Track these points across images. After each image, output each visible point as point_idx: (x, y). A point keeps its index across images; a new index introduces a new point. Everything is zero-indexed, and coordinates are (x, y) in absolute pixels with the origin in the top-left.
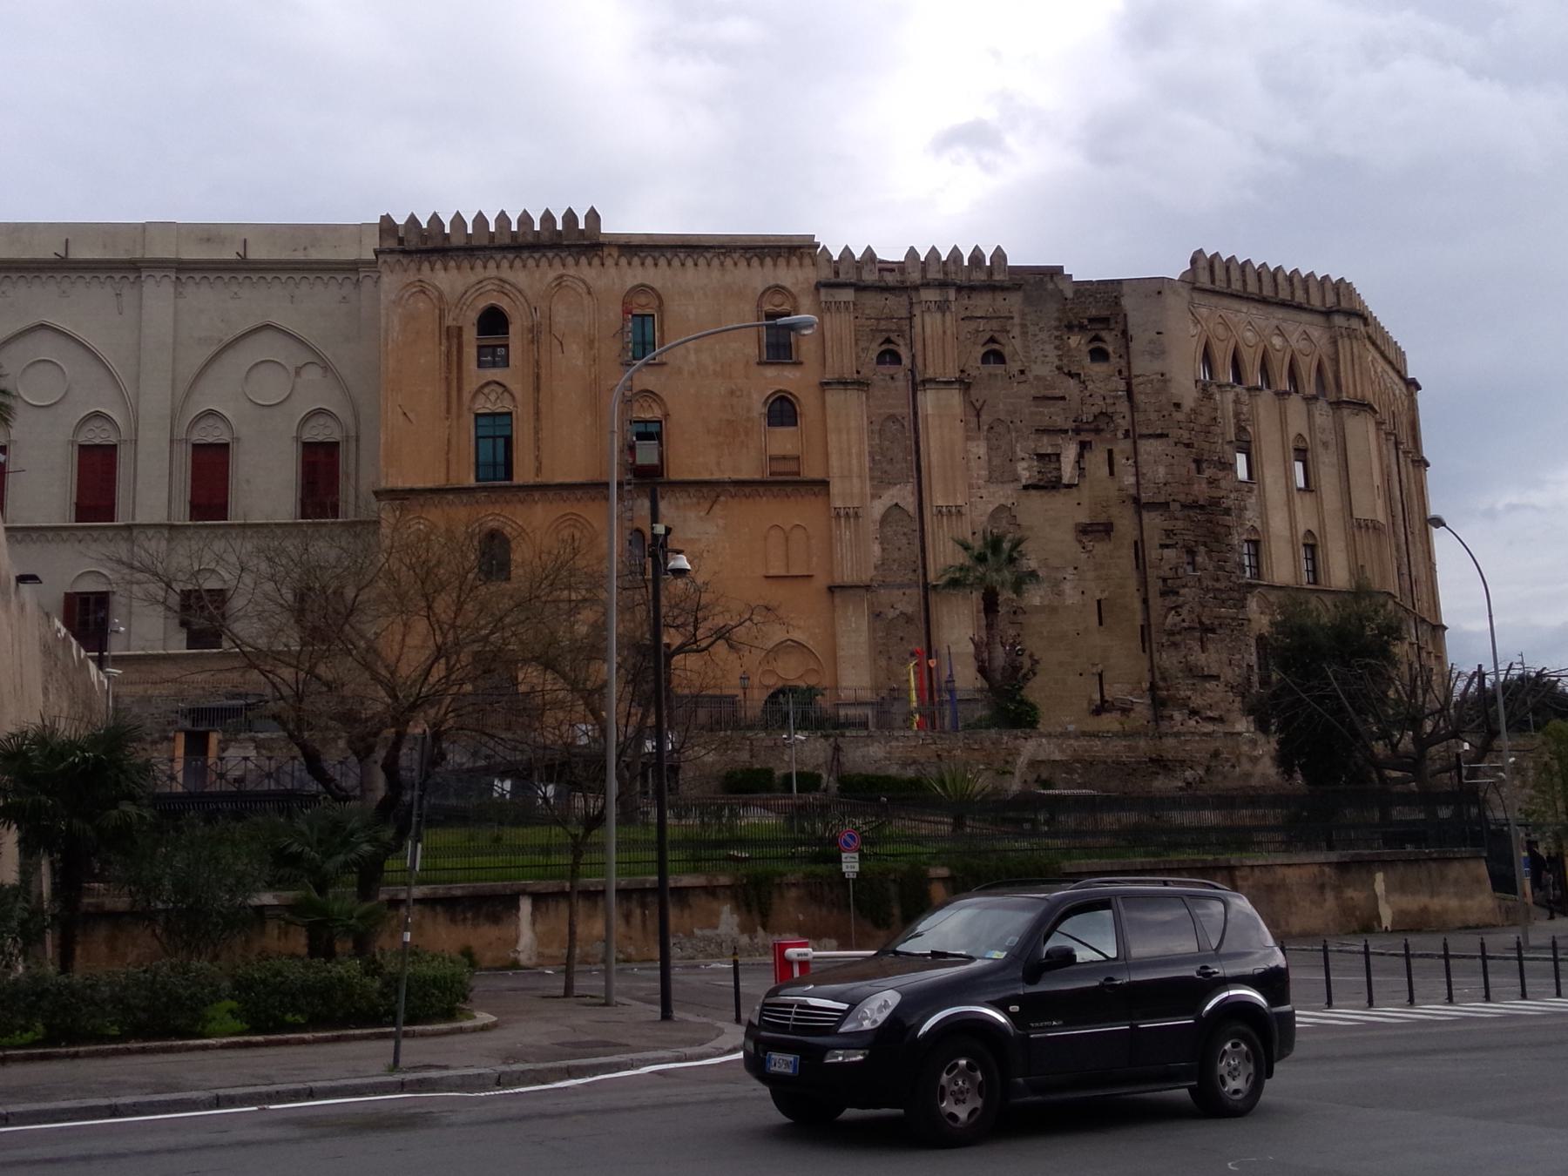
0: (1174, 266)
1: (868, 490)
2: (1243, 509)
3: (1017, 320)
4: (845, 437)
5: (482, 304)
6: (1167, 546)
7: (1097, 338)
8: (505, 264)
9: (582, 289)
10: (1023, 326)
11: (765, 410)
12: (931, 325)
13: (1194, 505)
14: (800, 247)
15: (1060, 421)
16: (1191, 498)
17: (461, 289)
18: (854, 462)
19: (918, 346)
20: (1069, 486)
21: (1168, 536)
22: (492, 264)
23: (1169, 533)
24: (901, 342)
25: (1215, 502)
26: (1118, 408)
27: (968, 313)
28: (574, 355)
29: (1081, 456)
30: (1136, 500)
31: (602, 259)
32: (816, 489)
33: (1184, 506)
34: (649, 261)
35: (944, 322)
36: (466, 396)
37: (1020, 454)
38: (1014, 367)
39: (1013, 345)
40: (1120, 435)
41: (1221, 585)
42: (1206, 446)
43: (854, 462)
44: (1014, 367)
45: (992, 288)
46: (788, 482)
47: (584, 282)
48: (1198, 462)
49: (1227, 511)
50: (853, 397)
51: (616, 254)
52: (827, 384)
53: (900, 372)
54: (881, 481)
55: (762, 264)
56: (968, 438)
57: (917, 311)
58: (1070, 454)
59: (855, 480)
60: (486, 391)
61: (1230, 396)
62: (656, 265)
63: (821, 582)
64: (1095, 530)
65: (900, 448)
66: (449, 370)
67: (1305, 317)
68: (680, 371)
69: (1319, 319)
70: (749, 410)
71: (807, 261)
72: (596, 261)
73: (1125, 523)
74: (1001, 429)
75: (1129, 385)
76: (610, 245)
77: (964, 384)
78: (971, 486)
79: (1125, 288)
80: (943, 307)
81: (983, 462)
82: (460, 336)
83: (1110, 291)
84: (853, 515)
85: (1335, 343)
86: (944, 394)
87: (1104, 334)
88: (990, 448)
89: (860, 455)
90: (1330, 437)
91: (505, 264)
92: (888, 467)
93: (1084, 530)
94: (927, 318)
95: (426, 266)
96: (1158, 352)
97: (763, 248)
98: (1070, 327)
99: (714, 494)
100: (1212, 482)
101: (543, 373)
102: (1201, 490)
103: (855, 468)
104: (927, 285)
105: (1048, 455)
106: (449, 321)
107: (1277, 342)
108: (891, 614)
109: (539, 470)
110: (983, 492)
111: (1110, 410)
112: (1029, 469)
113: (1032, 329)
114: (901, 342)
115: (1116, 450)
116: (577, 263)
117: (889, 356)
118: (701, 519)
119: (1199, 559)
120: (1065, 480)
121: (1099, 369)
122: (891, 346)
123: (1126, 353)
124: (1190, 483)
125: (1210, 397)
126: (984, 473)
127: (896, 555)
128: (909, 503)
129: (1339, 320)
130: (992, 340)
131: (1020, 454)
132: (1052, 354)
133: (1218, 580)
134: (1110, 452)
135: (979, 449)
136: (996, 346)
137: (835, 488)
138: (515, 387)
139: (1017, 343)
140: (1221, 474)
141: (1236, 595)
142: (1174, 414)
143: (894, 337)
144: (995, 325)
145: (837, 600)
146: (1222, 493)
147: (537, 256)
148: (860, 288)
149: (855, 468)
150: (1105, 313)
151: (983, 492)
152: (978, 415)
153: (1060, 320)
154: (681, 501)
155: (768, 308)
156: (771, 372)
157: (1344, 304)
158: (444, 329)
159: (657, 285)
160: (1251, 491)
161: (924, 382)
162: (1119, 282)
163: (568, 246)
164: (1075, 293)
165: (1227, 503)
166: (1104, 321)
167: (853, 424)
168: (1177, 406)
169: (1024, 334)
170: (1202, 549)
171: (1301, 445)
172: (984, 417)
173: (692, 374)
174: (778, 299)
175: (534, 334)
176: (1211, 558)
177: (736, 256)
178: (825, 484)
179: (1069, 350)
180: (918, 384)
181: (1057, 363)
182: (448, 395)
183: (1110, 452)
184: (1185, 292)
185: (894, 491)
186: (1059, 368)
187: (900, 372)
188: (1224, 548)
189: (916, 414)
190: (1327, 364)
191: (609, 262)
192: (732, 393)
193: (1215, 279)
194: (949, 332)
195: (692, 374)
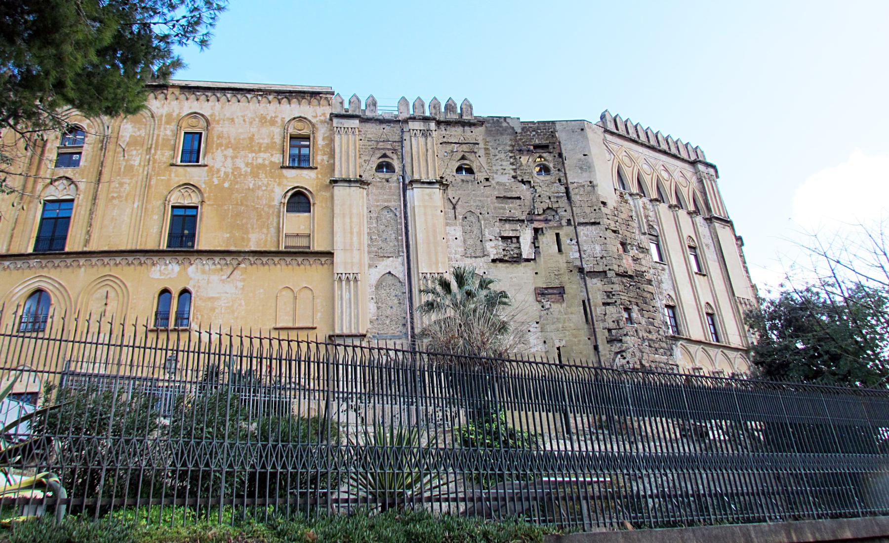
1: (366, 260)
2: (660, 282)
3: (482, 145)
4: (348, 220)
6: (608, 304)
10: (486, 149)
12: (416, 145)
13: (624, 275)
14: (319, 93)
16: (621, 270)
18: (355, 239)
19: (407, 160)
20: (528, 260)
21: (608, 296)
23: (609, 294)
24: (395, 157)
26: (560, 204)
27: (445, 140)
29: (535, 238)
30: (581, 270)
31: (166, 95)
32: (323, 260)
33: (617, 275)
37: (488, 236)
39: (478, 162)
40: (564, 222)
41: (654, 336)
42: (628, 234)
43: (355, 239)
44: (480, 176)
45: (462, 123)
48: (623, 244)
50: (355, 192)
52: (336, 181)
54: (379, 255)
56: (447, 224)
57: (406, 136)
58: (526, 236)
59: (356, 252)
60: (57, 183)
62: (208, 100)
64: (550, 293)
71: (323, 102)
73: (573, 286)
74: (472, 219)
75: (567, 189)
78: (450, 259)
79: (558, 127)
80: (426, 134)
81: (460, 241)
83: (548, 128)
85: (701, 181)
86: (428, 191)
89: (359, 234)
92: (383, 245)
93: (541, 293)
96: (586, 166)
97: (290, 92)
98: (520, 151)
100: (635, 260)
102: (627, 263)
104: (413, 119)
105: (511, 238)
109: (87, 242)
111: (555, 206)
112: (495, 247)
113: (492, 151)
115: (561, 233)
117: (385, 166)
118: (223, 281)
119: (635, 315)
120: (524, 256)
124: (620, 258)
126: (461, 250)
127: (389, 312)
128: (399, 270)
129: (701, 167)
132: (509, 168)
133: (650, 332)
134: (557, 235)
135: (456, 231)
137: (337, 258)
139: (483, 160)
140: (641, 256)
142: (602, 208)
143: (389, 153)
146: (644, 269)
148: (364, 120)
150: (544, 142)
152: (454, 208)
154: (207, 267)
155: (291, 130)
157: (700, 159)
161: (412, 182)
162: (553, 122)
164: (523, 129)
165: (648, 276)
166: (545, 147)
168: (604, 203)
169: (487, 154)
170: (635, 308)
174: (300, 125)
176: (643, 316)
177: (271, 97)
178: (330, 254)
179: (521, 165)
180: (407, 185)
183: (557, 235)
186: (514, 177)
188: (652, 309)
190: (698, 194)
193: (616, 130)
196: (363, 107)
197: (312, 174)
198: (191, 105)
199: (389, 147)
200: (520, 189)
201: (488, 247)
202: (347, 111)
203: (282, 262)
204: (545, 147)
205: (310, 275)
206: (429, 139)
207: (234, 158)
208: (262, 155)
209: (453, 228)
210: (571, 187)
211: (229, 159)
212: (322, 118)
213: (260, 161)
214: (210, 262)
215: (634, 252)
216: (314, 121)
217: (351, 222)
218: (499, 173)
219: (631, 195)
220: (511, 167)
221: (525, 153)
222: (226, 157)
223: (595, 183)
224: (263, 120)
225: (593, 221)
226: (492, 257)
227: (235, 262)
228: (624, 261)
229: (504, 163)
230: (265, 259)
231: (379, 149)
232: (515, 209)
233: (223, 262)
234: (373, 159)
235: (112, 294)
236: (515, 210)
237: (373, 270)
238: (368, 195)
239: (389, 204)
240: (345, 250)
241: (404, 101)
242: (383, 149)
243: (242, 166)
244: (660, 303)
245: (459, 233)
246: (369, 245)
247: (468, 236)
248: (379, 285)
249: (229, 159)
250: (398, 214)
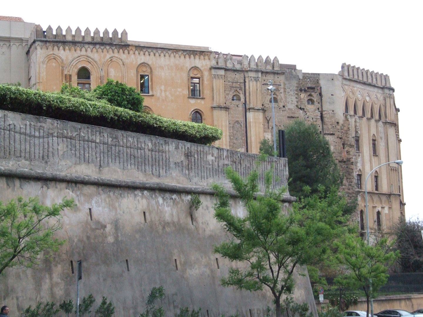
2: (357, 163)
3: (282, 86)
5: (80, 66)
7: (310, 95)
8: (89, 50)
9: (121, 63)
10: (285, 89)
12: (252, 86)
14: (204, 52)
17: (70, 59)
22: (83, 49)
24: (241, 92)
25: (349, 160)
27: (265, 82)
33: (340, 162)
34: (147, 53)
38: (281, 105)
39: (281, 96)
41: (351, 191)
47: (121, 60)
48: (343, 144)
49: (352, 163)
50: (223, 113)
51: (134, 50)
52: (214, 107)
53: (241, 104)
55: (190, 58)
56: (265, 131)
57: (247, 80)
61: (353, 120)
62: (149, 55)
67: (376, 90)
68: (159, 99)
69: (380, 91)
72: (126, 51)
75: (322, 114)
76: (132, 46)
79: (321, 77)
80: (256, 79)
82: (70, 79)
83: (315, 78)
85: (385, 99)
86: (257, 114)
87: (313, 94)
90: (382, 135)
91: (89, 50)
95: (56, 48)
98: (301, 90)
104: (251, 71)
106: (66, 72)
107: (368, 99)
113: (288, 90)
114: (241, 92)
116: (119, 52)
117: (235, 97)
122: (237, 94)
125: (348, 120)
129: (386, 91)
132: (295, 100)
133: (349, 189)
139: (282, 95)
140: (351, 149)
141: (354, 195)
142: (337, 126)
143: (238, 90)
146: (351, 156)
147: (102, 47)
150: (313, 86)
152: (268, 123)
153: (297, 87)
155: (192, 75)
156: (192, 101)
157: (388, 85)
158: (64, 76)
159: (150, 63)
160: (359, 156)
161: (249, 109)
162: (319, 74)
163: (115, 45)
164: (303, 77)
167: (224, 124)
168: (338, 123)
169: (285, 91)
171: (374, 138)
172: (270, 124)
174: (196, 72)
177: (180, 53)
179: (301, 99)
181: (296, 104)
184: (340, 78)
186: (297, 106)
190: (382, 107)
191: (131, 52)
194: (258, 90)
197: (203, 102)
199: (238, 86)
206: (258, 82)
208: (179, 90)
209: (267, 133)
210: (324, 113)
211: (163, 92)
212: (206, 67)
213: (178, 93)
215: (347, 149)
216: (202, 69)
219: (350, 116)
221: (303, 91)
222: (161, 90)
223: (335, 112)
225: (332, 133)
228: (343, 154)
231: (233, 87)
234: (231, 93)
239: (238, 120)
242: (235, 87)
244: (355, 174)
246: (229, 141)
249: (163, 92)
250: (242, 125)
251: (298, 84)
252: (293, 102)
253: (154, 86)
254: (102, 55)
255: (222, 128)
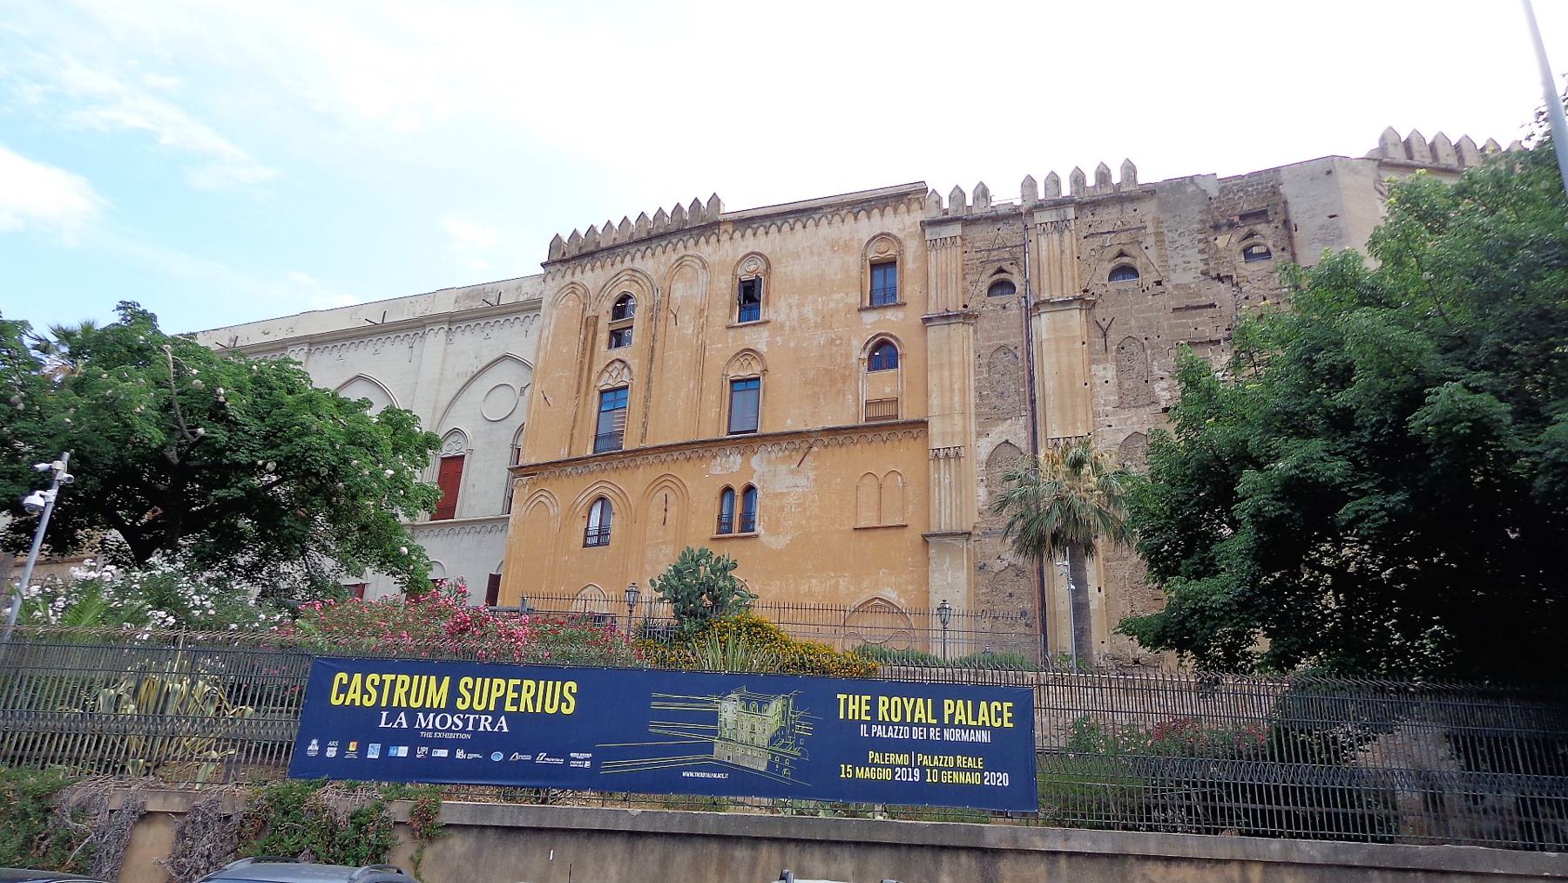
0: (1359, 144)
3: (1150, 229)
4: (946, 373)
5: (616, 293)
9: (697, 265)
10: (1159, 234)
11: (865, 356)
12: (1045, 247)
14: (907, 194)
15: (1208, 332)
18: (956, 399)
19: (1032, 272)
22: (628, 258)
24: (1015, 270)
27: (1092, 230)
28: (687, 326)
32: (915, 432)
35: (1061, 241)
36: (594, 377)
39: (1147, 257)
43: (956, 399)
44: (1148, 279)
45: (1121, 198)
46: (885, 425)
47: (700, 258)
50: (959, 331)
52: (929, 320)
54: (989, 416)
56: (1092, 362)
59: (958, 420)
63: (916, 531)
65: (1015, 383)
66: (584, 355)
68: (782, 327)
70: (848, 356)
71: (915, 206)
72: (713, 239)
74: (1134, 348)
77: (1085, 301)
79: (1284, 176)
80: (1060, 227)
84: (954, 456)
88: (1120, 371)
89: (963, 391)
92: (996, 402)
94: (1043, 241)
97: (868, 200)
98: (1217, 227)
99: (805, 446)
101: (658, 346)
103: (957, 407)
106: (589, 313)
108: (998, 566)
109: (644, 436)
110: (1113, 420)
113: (1169, 236)
117: (1001, 286)
118: (792, 472)
121: (1255, 267)
123: (1289, 245)
126: (1114, 398)
128: (1021, 439)
130: (1122, 254)
131: (1158, 373)
136: (1125, 260)
137: (935, 427)
138: (634, 363)
139: (1152, 254)
144: (1124, 238)
145: (932, 552)
148: (969, 222)
149: (957, 407)
150: (1260, 206)
151: (1113, 420)
155: (872, 255)
156: (870, 318)
162: (1277, 170)
164: (1221, 190)
166: (1261, 215)
172: (1112, 336)
173: (793, 329)
174: (883, 246)
175: (654, 314)
178: (923, 424)
179: (1217, 251)
180: (1032, 309)
181: (1202, 267)
182: (580, 376)
185: (1005, 426)
187: (1012, 301)
189: (1029, 341)
191: (725, 237)
192: (833, 340)
195: (793, 329)
196: (969, 202)
198: (750, 242)
199: (1007, 256)
200: (1215, 290)
201: (1157, 389)
202: (946, 212)
203: (863, 440)
204: (1261, 215)
205: (897, 456)
207: (800, 306)
208: (836, 296)
213: (832, 305)
214: (776, 448)
217: (951, 374)
218: (1179, 270)
220: (1200, 256)
221: (1225, 229)
224: (833, 245)
226: (1163, 404)
227: (805, 446)
229: (1188, 252)
230: (840, 438)
232: (1204, 324)
233: (791, 446)
234: (984, 277)
235: (671, 498)
236: (1205, 326)
237: (983, 442)
238: (975, 332)
240: (942, 416)
241: (1029, 183)
243: (810, 315)
245: (1110, 372)
247: (1125, 376)
248: (991, 461)
251: (1208, 211)
252: (1192, 265)
253: (771, 299)
254: (663, 259)
255: (951, 370)
